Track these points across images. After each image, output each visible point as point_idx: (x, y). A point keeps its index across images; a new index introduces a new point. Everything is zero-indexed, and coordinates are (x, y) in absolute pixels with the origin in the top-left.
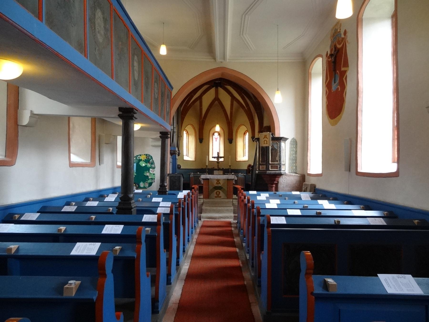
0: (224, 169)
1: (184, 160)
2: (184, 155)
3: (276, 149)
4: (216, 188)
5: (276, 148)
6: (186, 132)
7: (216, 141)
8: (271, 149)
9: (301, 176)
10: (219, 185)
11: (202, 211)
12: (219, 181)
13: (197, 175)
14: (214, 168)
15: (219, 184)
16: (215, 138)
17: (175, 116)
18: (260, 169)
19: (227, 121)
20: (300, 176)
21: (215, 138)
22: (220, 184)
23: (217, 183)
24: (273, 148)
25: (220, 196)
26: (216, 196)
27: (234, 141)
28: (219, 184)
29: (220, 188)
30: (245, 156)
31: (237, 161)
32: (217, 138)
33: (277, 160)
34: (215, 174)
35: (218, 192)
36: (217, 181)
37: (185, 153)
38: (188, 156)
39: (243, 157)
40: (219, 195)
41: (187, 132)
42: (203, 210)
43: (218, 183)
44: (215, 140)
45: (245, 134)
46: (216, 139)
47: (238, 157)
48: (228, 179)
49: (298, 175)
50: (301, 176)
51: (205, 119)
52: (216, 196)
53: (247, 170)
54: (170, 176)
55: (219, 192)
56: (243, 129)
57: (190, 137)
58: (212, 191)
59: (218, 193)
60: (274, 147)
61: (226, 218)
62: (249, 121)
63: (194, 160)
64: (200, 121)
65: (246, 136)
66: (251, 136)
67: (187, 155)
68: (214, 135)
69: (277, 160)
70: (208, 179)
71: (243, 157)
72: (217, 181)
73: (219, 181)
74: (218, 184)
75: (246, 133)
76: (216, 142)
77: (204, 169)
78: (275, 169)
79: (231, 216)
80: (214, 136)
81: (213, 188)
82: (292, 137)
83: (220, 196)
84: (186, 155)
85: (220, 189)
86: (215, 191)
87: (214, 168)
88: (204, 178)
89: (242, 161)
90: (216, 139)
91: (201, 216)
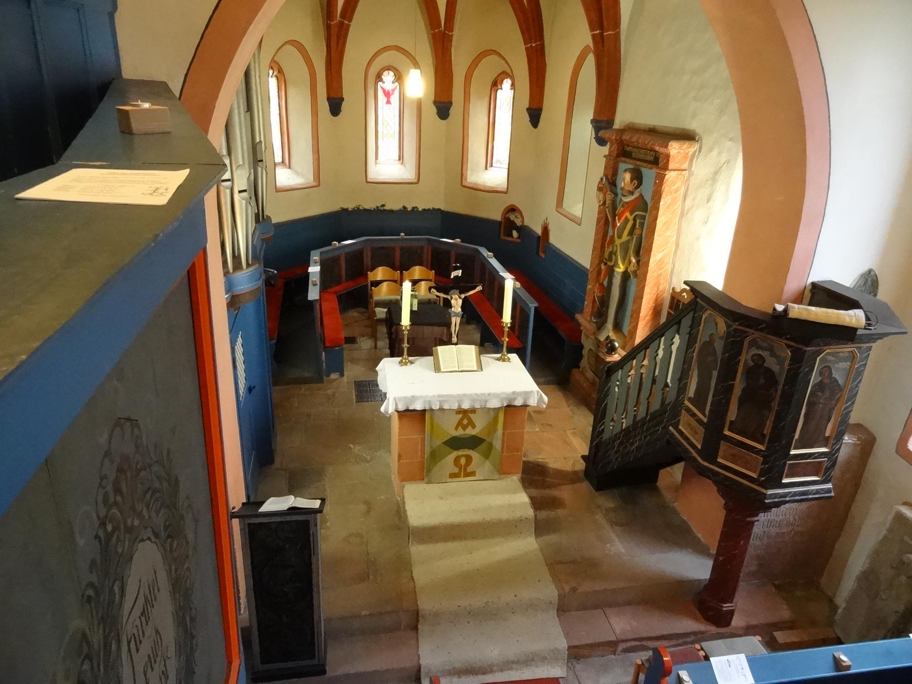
0: (420, 209)
1: (278, 190)
2: (276, 161)
3: (839, 385)
4: (455, 443)
5: (838, 378)
6: (275, 73)
7: (388, 102)
8: (813, 387)
9: (859, 442)
10: (470, 431)
11: (418, 621)
12: (472, 416)
13: (330, 255)
14: (383, 206)
15: (470, 427)
16: (384, 90)
17: (236, 111)
18: (720, 460)
19: (433, 28)
20: (855, 444)
21: (384, 90)
22: (474, 426)
23: (460, 424)
24: (826, 381)
25: (469, 470)
26: (456, 470)
27: (456, 111)
28: (470, 427)
29: (474, 442)
30: (492, 166)
31: (466, 184)
32: (393, 90)
33: (827, 434)
34: (442, 370)
35: (463, 456)
36: (460, 416)
37: (278, 159)
38: (290, 168)
39: (486, 169)
40: (465, 470)
41: (280, 71)
42: (420, 619)
43: (465, 422)
44: (386, 99)
45: (496, 84)
46: (387, 94)
47: (468, 172)
48: (509, 408)
49: (850, 441)
50: (859, 442)
51: (350, 20)
52: (456, 470)
53: (500, 222)
54: (249, 524)
55: (469, 459)
56: (489, 67)
57: (291, 92)
58: (435, 457)
59: (463, 461)
60: (831, 373)
61: (533, 660)
62: (525, 43)
63: (314, 184)
64: (328, 28)
65: (499, 92)
66: (528, 107)
67: (287, 162)
68: (381, 80)
69: (827, 434)
70: (424, 412)
71: (486, 169)
72: (460, 416)
73: (472, 416)
74: (464, 428)
75: (502, 82)
76: (388, 105)
77: (352, 211)
78: (805, 475)
79: (555, 651)
80: (380, 83)
81: (445, 443)
82: (864, 269)
83: (469, 470)
84: (283, 162)
85: (473, 449)
86: (450, 453)
87: (385, 208)
88: (401, 408)
89: (482, 188)
90: (387, 94)
91: (422, 670)
